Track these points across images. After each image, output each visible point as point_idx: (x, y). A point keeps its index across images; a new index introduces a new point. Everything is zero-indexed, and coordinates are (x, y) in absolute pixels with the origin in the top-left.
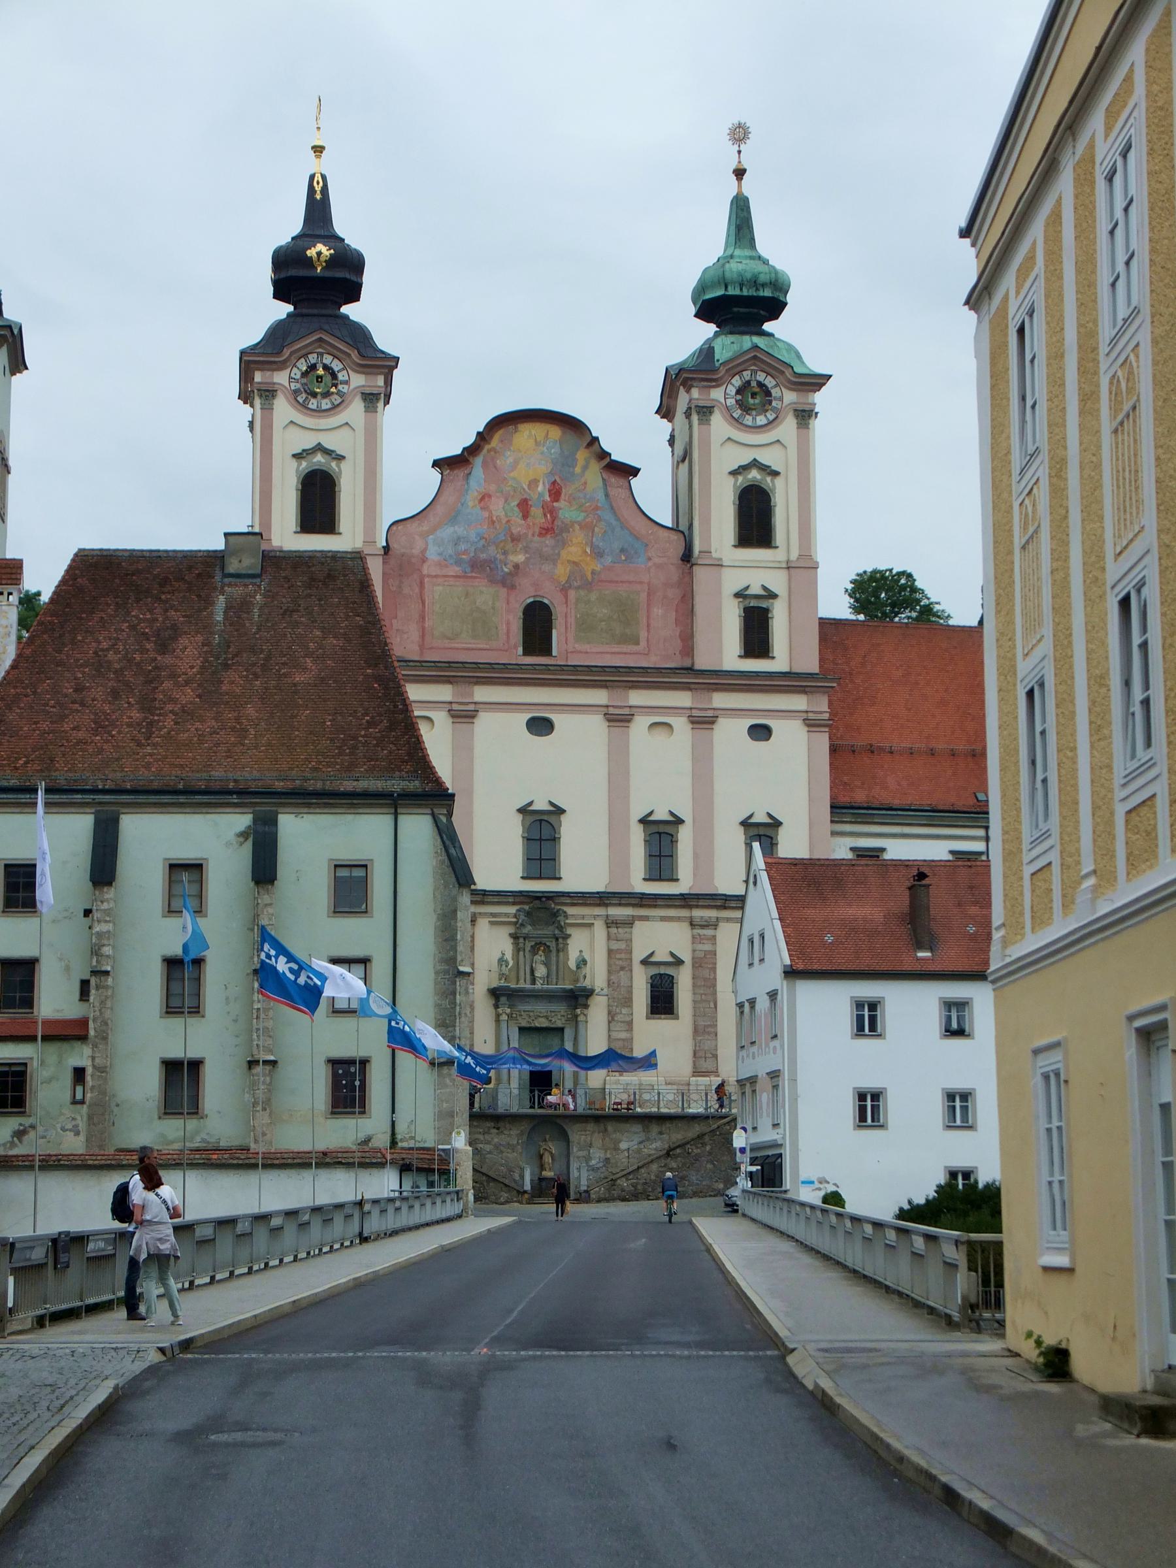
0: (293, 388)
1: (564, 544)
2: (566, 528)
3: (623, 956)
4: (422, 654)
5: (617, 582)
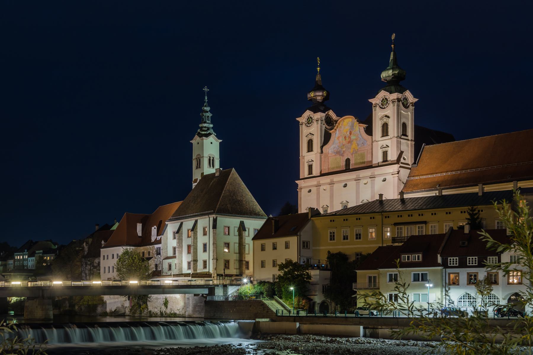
1: (352, 144)
2: (352, 141)
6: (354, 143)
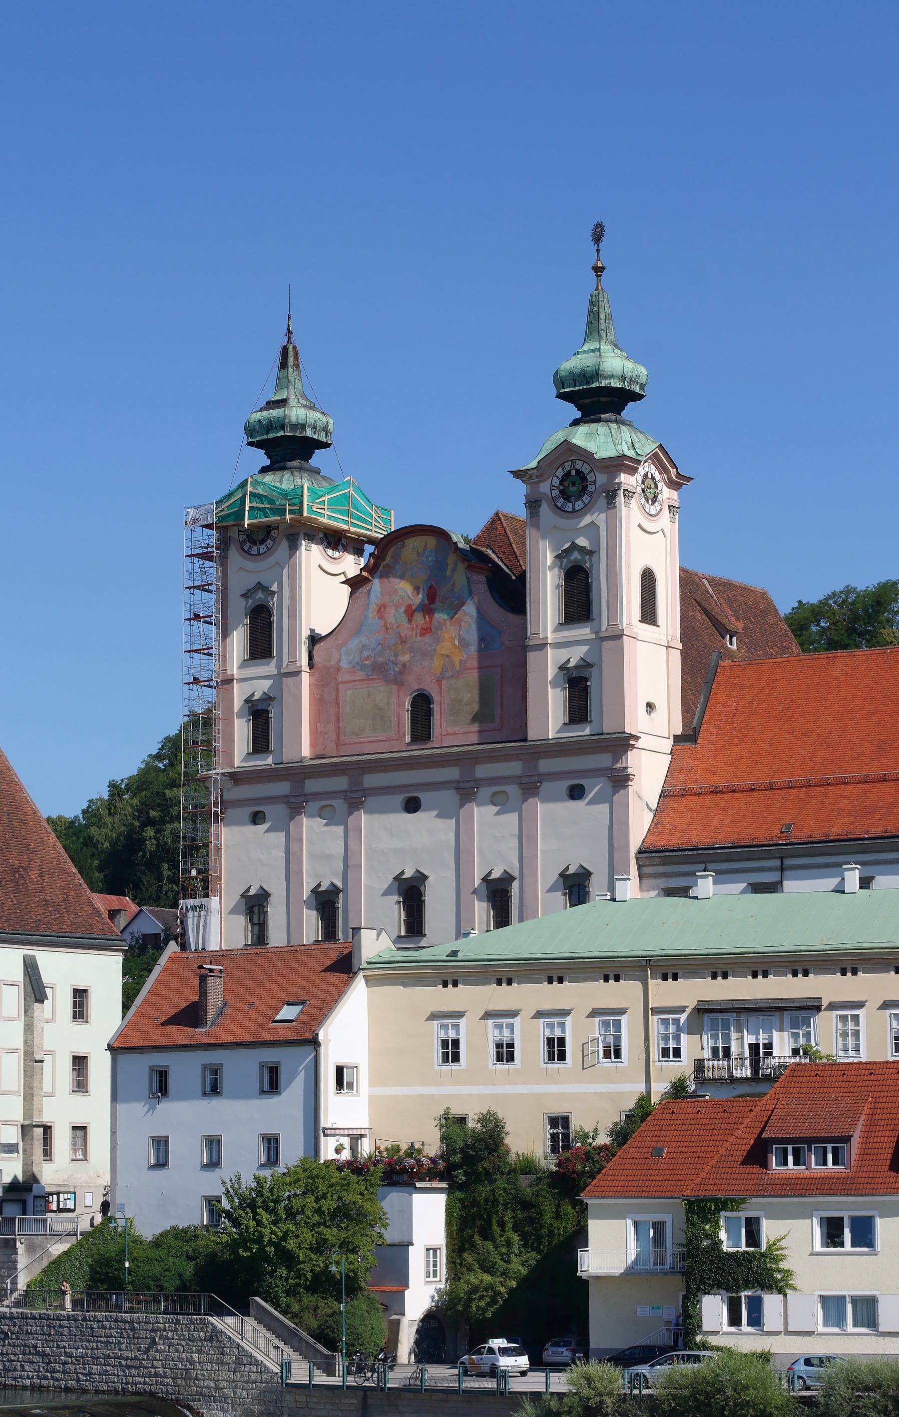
0: (241, 539)
1: (438, 640)
4: (337, 750)
6: (446, 636)
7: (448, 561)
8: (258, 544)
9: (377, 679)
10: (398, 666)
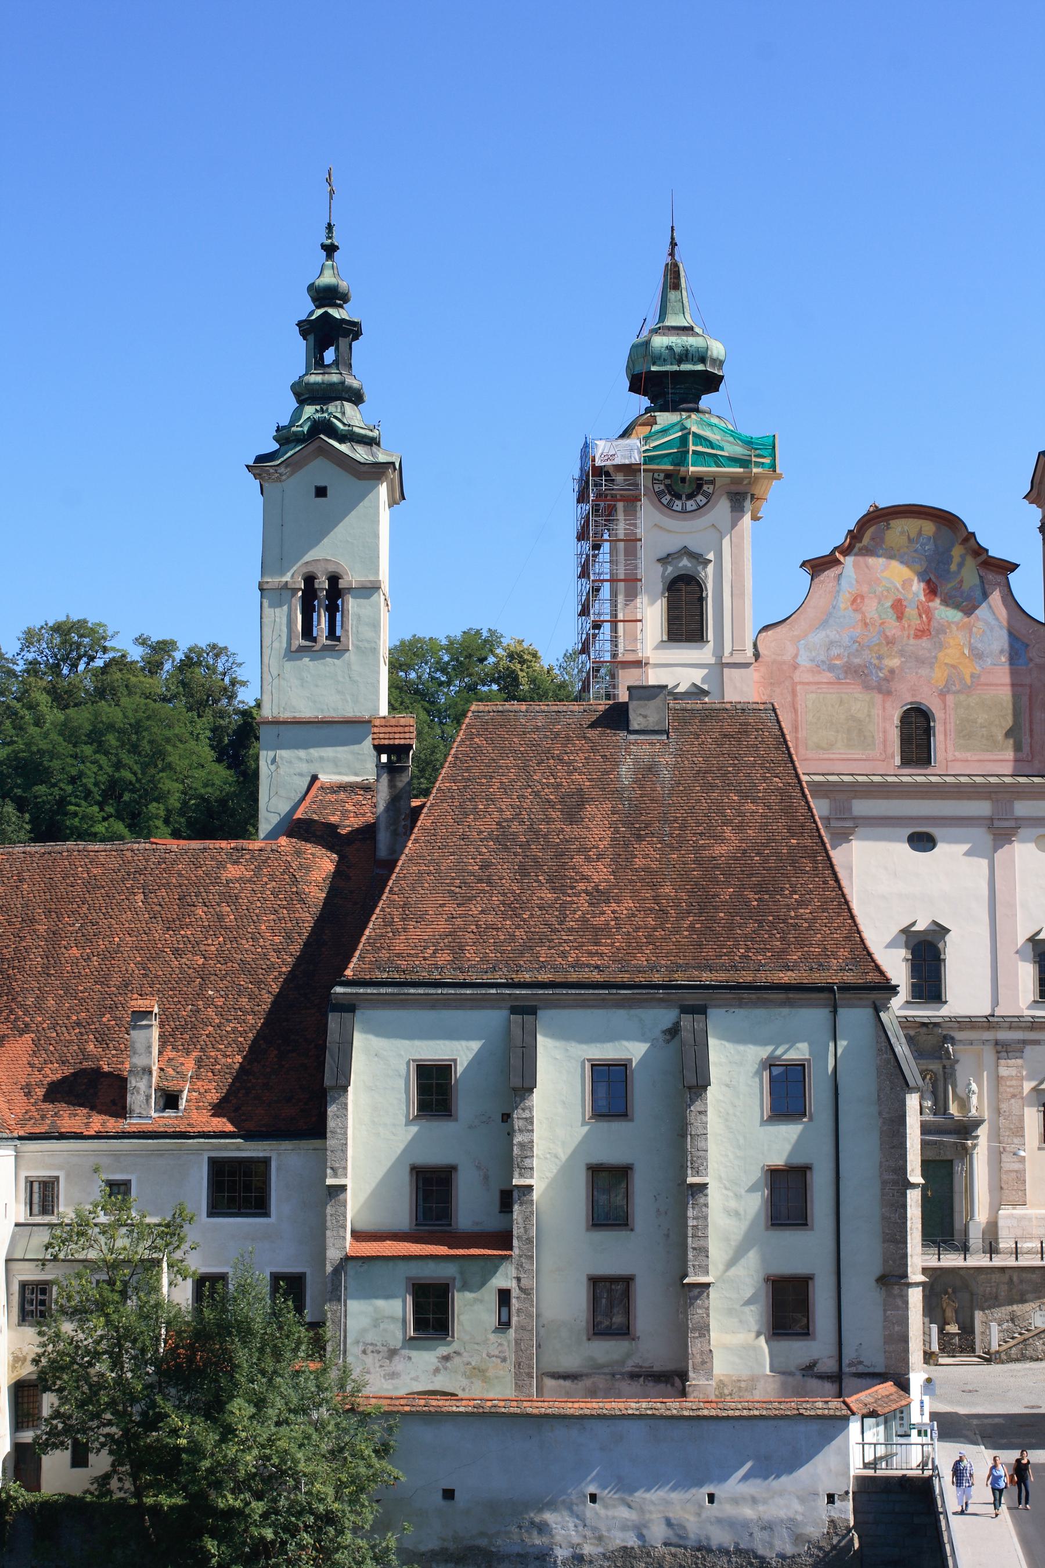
0: (657, 490)
1: (941, 646)
2: (942, 630)
3: (1014, 1083)
5: (997, 685)
7: (953, 553)
8: (684, 497)
9: (853, 684)
10: (883, 671)
